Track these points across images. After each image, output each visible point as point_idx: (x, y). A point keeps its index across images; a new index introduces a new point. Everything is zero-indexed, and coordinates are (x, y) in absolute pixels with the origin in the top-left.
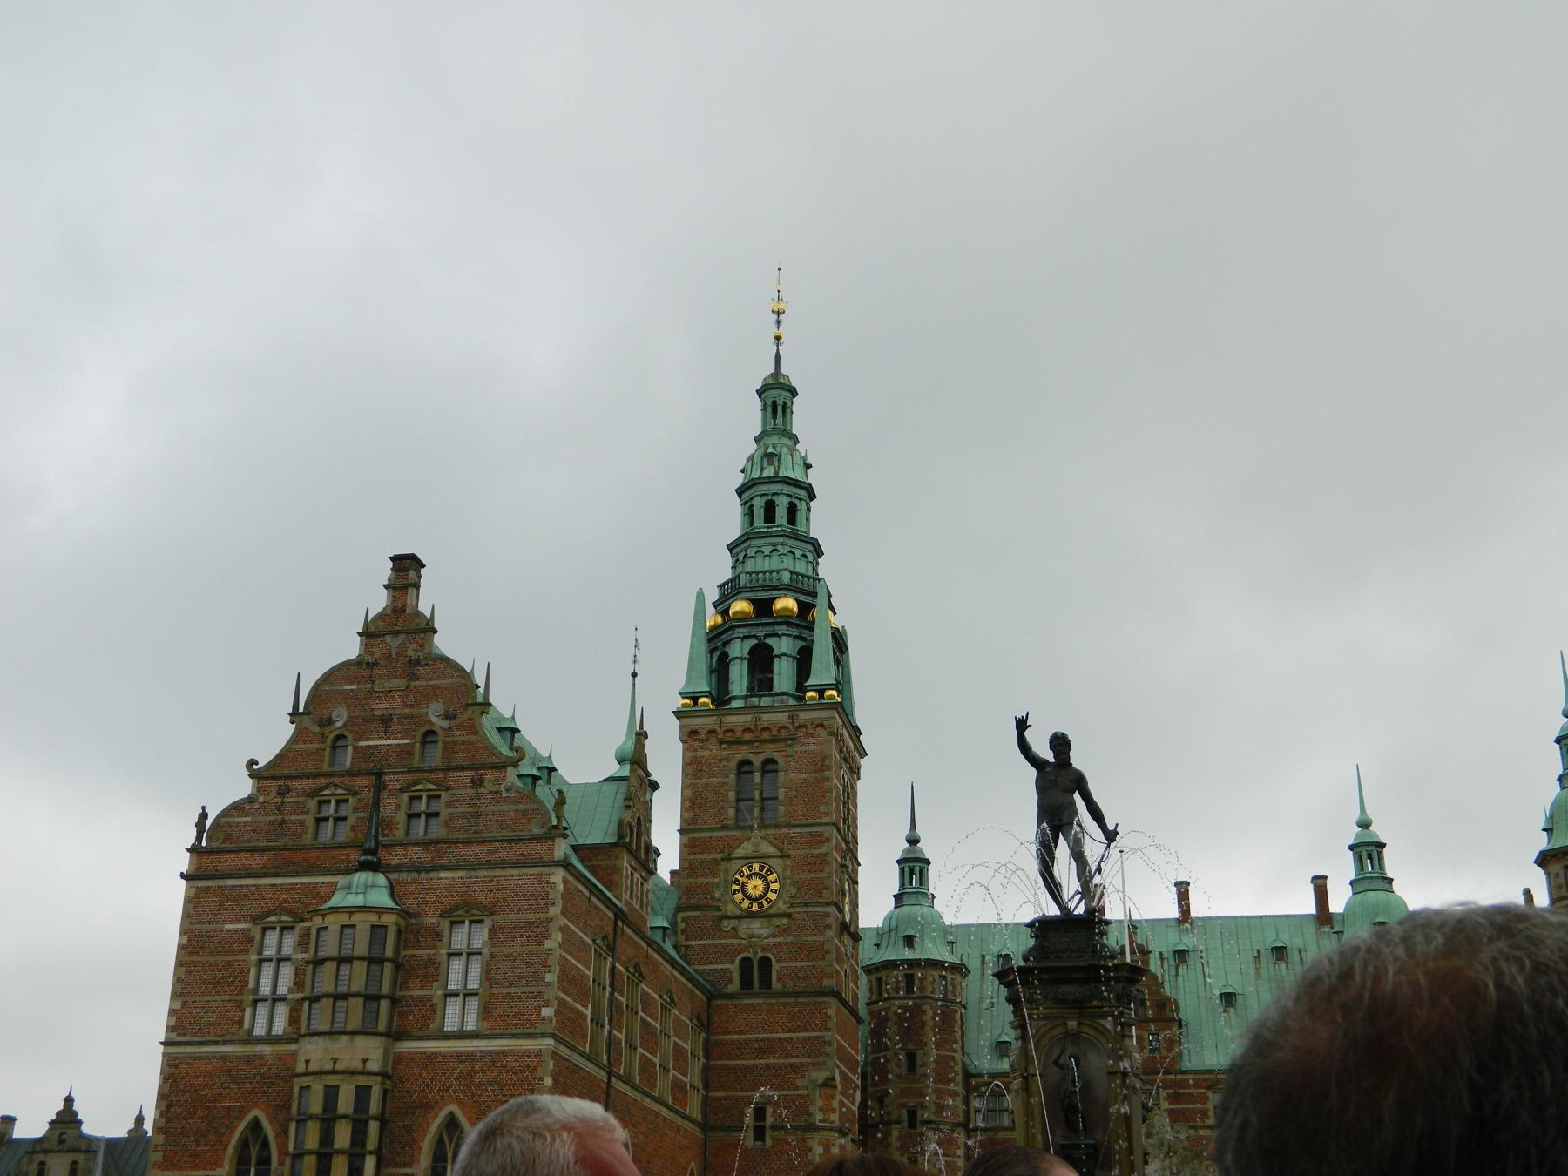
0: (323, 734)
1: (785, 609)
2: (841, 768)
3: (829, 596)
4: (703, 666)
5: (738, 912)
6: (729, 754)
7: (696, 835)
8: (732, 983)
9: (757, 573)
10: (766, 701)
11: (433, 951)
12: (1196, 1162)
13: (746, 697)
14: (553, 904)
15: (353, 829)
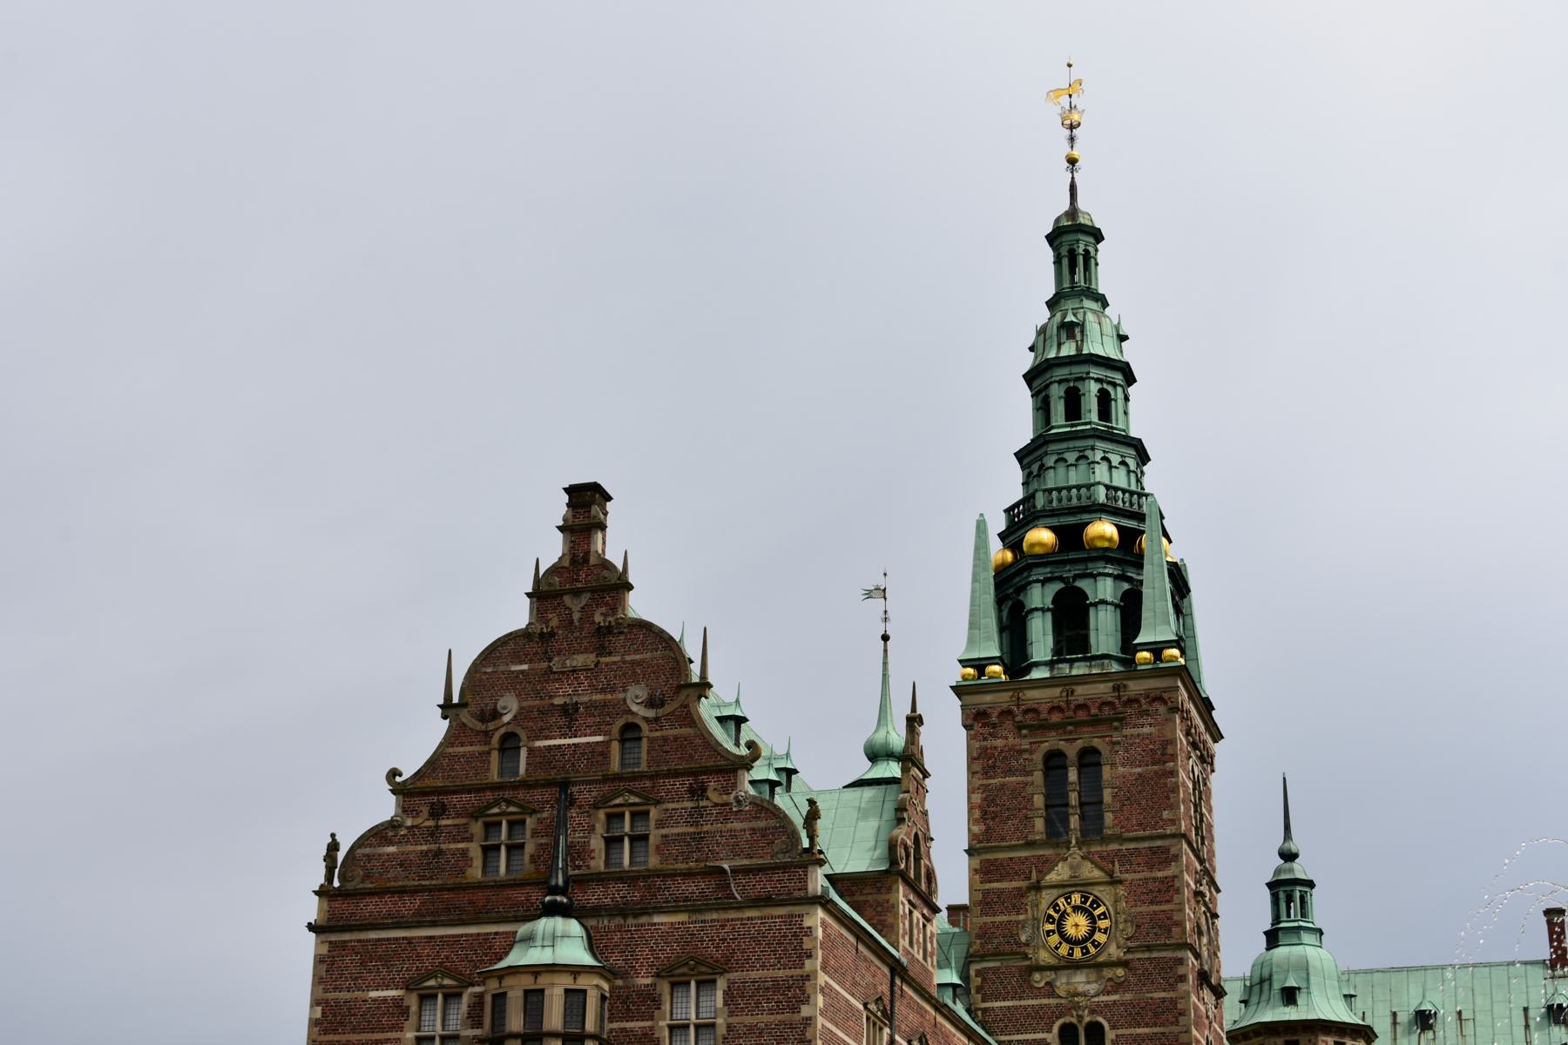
0: (486, 733)
1: (1102, 538)
2: (1190, 757)
3: (1162, 517)
4: (990, 623)
5: (1052, 961)
7: (988, 856)
9: (1059, 490)
10: (1079, 670)
11: (648, 1024)
13: (1051, 664)
14: (810, 956)
15: (533, 859)
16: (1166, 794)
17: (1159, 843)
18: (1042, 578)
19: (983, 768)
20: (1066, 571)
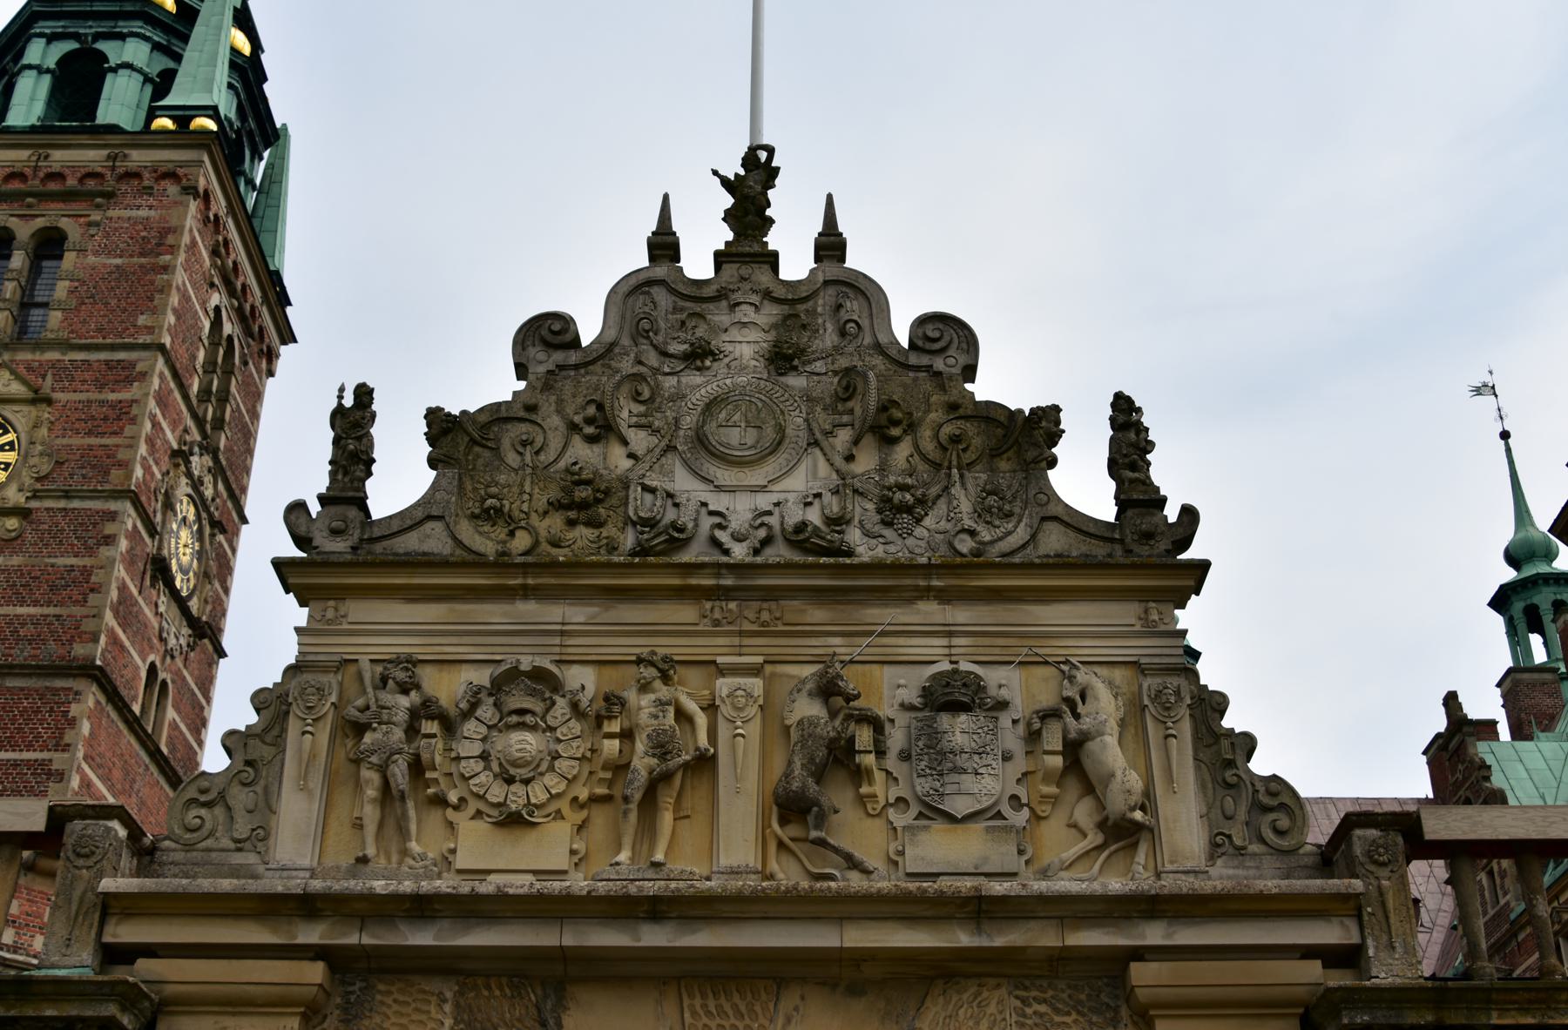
12: (1003, 465)
16: (149, 294)
17: (122, 355)
18: (47, 31)
20: (85, 27)
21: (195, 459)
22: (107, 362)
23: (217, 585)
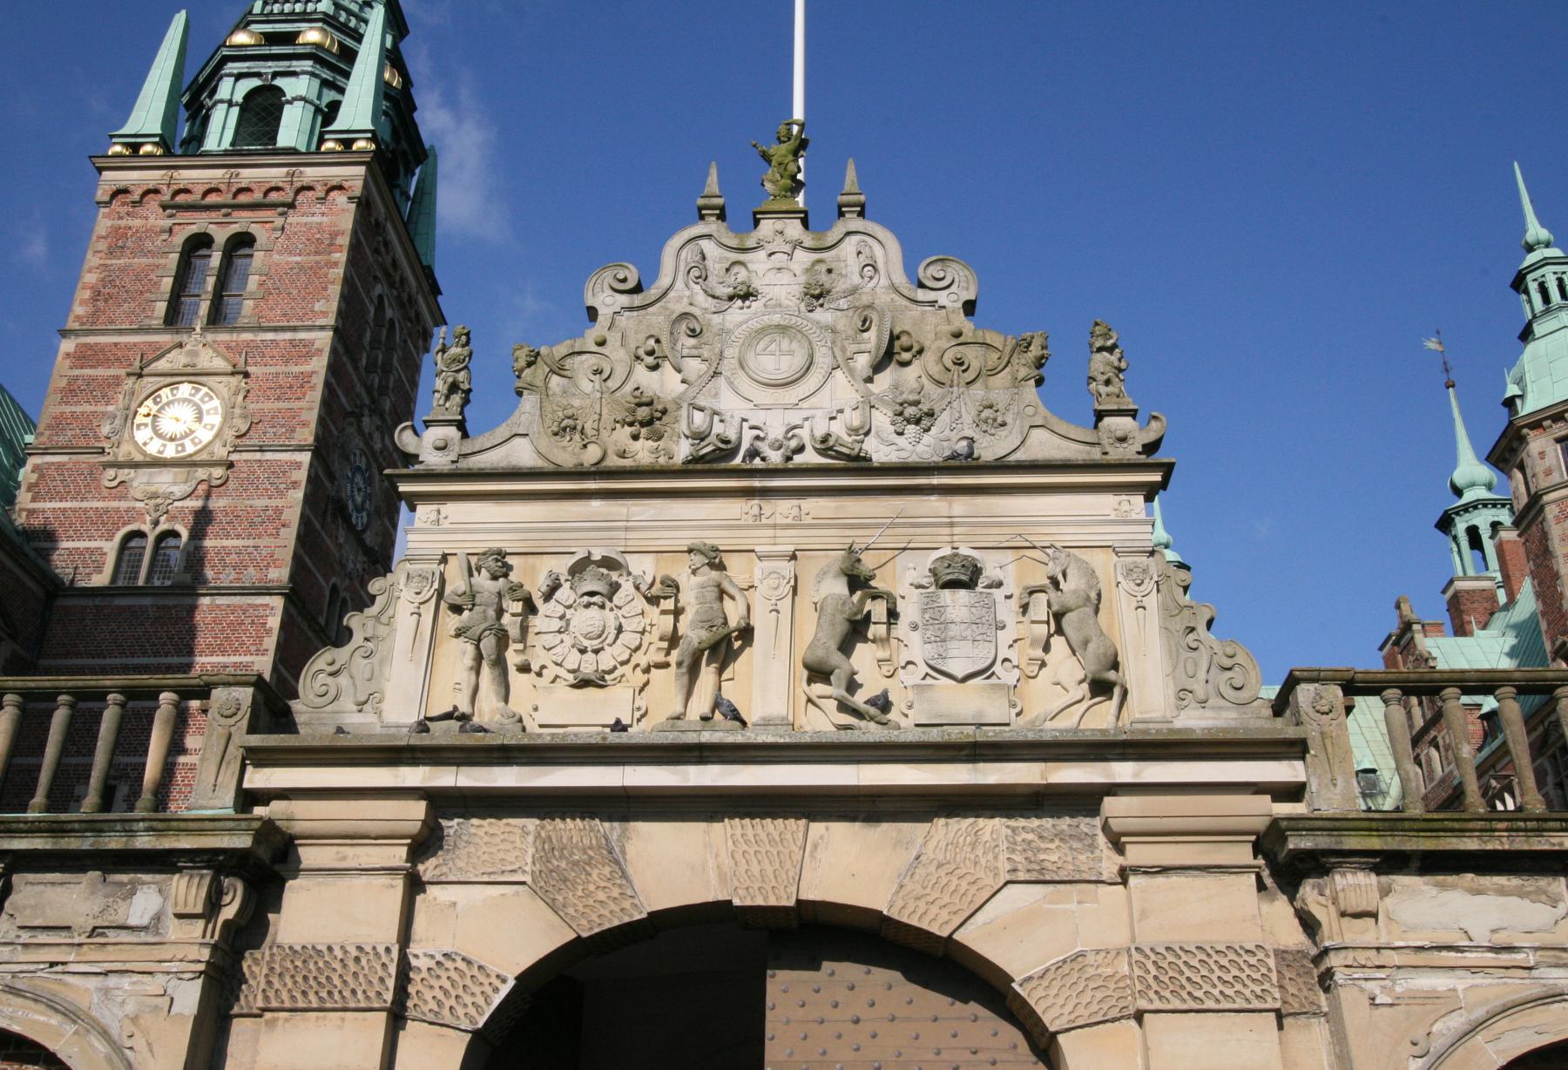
5: (139, 458)
6: (174, 224)
8: (100, 572)
17: (302, 335)
19: (110, 247)
21: (366, 420)
22: (291, 341)
23: (387, 522)
